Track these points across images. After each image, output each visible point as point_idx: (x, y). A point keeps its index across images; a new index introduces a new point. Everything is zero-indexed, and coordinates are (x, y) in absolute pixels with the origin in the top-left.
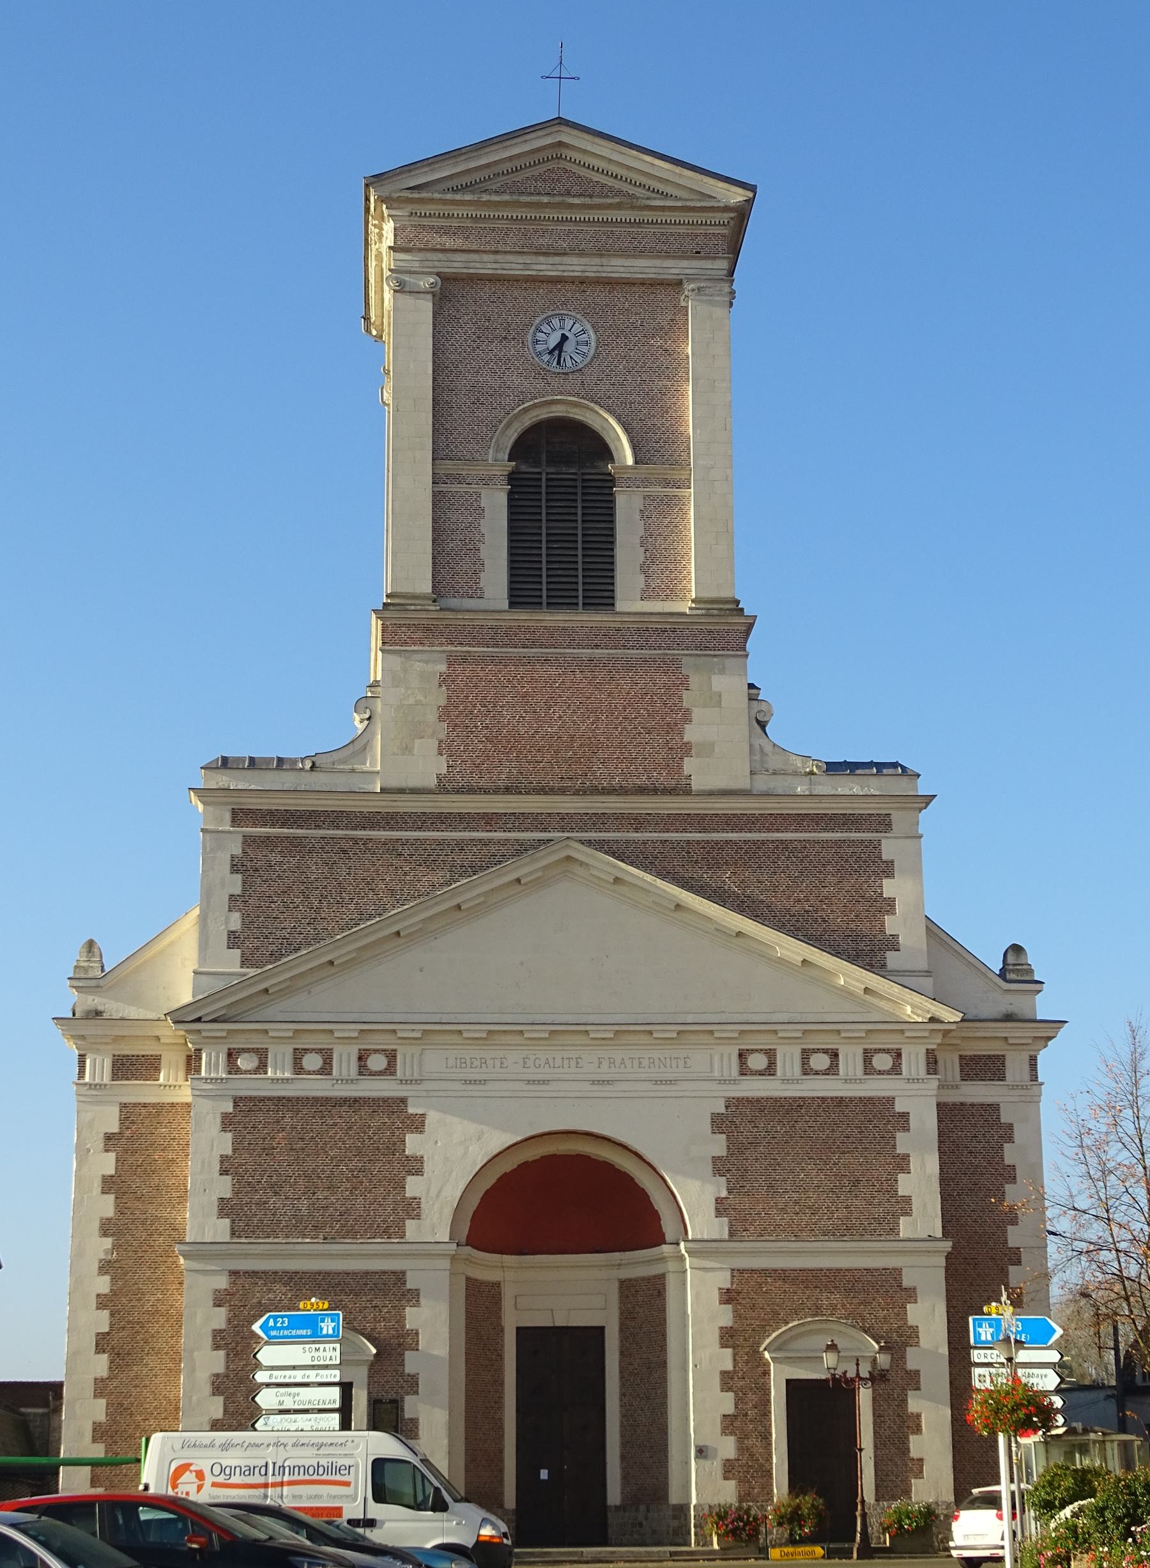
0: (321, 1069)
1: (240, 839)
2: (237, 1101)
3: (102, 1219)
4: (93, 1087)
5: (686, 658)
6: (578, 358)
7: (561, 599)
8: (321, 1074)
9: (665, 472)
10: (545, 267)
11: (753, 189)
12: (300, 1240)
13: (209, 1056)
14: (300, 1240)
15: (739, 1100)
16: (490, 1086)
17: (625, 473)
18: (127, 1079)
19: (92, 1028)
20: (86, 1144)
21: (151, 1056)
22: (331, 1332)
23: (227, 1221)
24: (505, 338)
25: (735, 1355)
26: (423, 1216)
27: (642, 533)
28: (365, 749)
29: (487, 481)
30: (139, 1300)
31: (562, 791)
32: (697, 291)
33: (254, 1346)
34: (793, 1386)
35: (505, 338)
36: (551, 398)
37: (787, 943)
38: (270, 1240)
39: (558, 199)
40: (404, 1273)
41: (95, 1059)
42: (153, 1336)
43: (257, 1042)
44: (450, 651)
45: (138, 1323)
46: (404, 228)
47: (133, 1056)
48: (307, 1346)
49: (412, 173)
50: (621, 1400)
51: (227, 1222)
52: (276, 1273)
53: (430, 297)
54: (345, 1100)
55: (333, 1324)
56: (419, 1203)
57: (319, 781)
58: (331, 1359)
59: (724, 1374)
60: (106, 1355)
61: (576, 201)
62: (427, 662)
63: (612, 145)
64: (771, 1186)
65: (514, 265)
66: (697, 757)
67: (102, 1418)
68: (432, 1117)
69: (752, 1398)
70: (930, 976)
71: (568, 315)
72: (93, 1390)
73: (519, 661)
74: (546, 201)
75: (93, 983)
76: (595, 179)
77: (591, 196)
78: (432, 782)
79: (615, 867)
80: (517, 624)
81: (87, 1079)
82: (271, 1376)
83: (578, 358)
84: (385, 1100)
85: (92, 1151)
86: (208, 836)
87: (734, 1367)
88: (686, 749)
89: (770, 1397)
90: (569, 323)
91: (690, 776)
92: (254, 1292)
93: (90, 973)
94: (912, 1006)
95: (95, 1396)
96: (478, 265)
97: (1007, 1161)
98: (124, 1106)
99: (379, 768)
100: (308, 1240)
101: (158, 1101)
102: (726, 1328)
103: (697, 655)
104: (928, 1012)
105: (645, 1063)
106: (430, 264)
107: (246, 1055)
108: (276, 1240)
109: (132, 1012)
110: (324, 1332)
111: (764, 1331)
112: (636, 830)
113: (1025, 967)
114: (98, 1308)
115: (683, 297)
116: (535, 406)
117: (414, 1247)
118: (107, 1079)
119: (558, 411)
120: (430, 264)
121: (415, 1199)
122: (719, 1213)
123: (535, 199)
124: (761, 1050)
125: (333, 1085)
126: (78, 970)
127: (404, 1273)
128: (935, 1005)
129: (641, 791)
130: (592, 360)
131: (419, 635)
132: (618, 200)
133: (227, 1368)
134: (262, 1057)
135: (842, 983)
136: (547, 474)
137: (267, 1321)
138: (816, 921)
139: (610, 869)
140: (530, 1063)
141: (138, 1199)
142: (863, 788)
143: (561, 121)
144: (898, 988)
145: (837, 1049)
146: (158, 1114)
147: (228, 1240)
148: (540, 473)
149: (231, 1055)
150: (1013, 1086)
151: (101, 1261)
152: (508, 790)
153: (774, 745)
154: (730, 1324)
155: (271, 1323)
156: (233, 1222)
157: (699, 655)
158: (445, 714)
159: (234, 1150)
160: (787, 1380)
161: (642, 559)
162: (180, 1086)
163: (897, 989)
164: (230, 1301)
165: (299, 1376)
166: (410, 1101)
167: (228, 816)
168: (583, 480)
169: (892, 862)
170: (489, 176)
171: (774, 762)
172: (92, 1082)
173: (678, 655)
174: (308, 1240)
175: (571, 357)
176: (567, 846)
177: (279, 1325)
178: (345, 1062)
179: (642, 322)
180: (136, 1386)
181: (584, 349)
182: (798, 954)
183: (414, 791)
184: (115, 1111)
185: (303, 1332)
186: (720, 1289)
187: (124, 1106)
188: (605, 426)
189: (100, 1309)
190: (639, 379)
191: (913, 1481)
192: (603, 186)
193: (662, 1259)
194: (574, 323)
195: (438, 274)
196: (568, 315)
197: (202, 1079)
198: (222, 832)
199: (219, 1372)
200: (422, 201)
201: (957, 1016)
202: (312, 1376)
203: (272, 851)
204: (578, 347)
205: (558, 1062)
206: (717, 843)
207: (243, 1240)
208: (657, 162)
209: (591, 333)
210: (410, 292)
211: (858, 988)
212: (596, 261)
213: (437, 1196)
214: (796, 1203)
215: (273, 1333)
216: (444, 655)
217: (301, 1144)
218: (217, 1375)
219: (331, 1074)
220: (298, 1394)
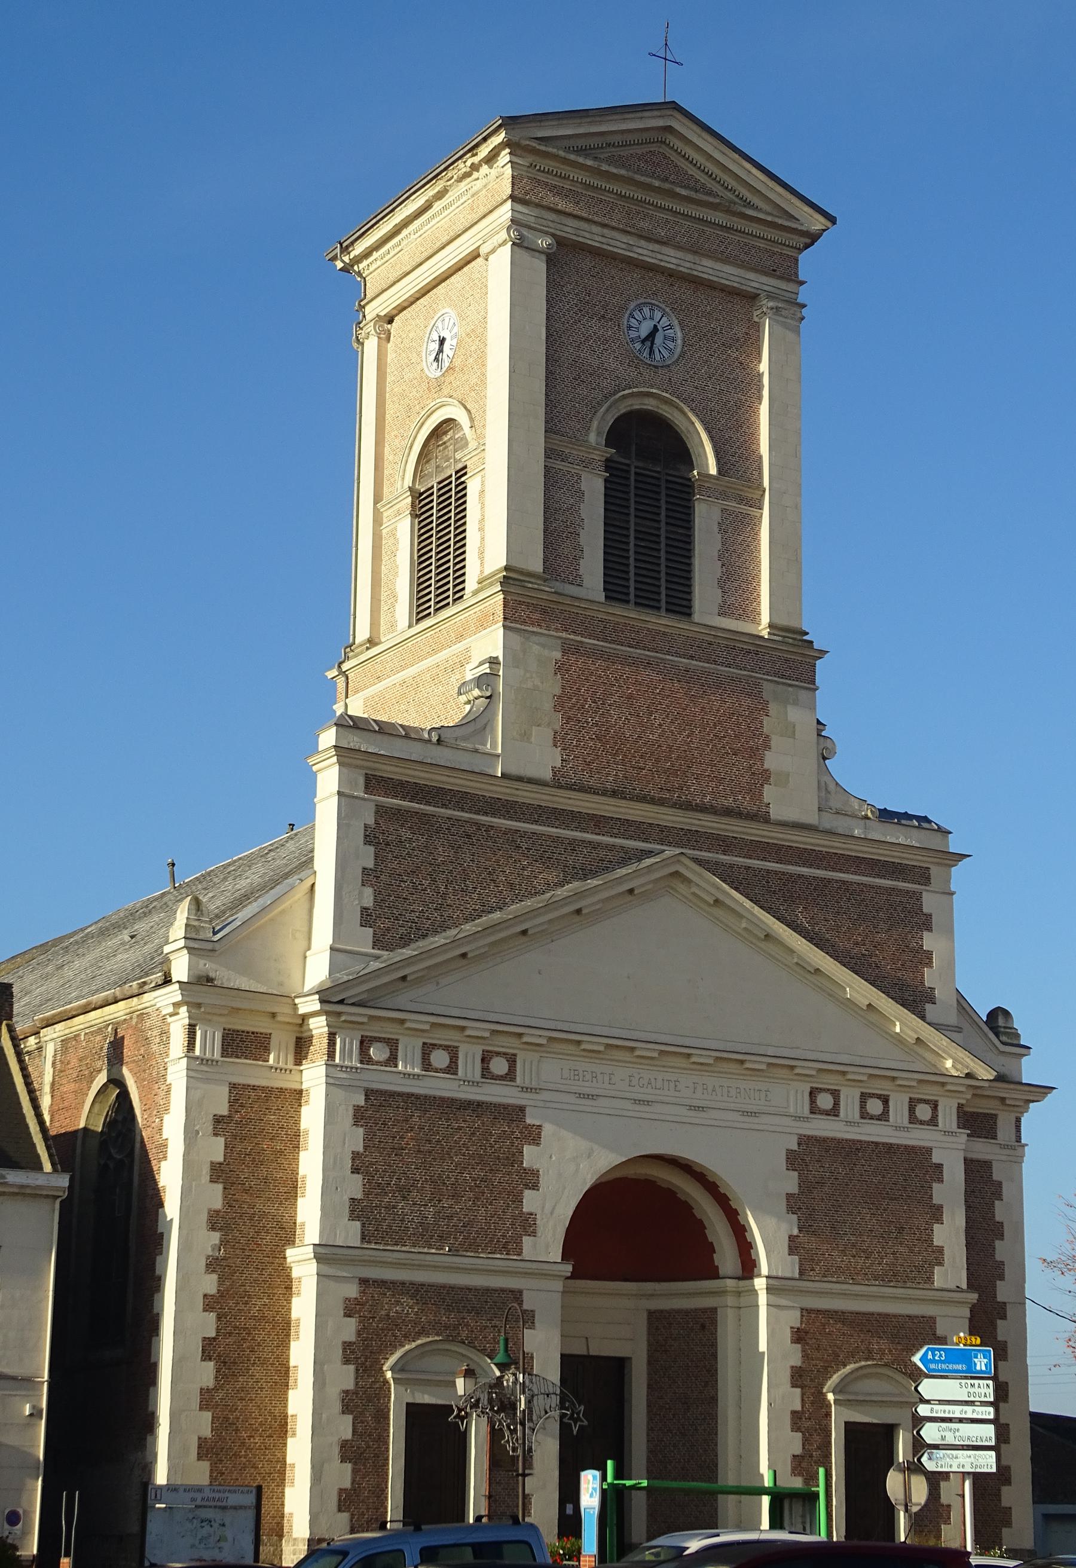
0: (447, 1067)
1: (372, 808)
2: (369, 1093)
3: (210, 1210)
4: (204, 1062)
5: (769, 683)
6: (666, 353)
7: (647, 601)
8: (448, 1073)
9: (741, 488)
10: (645, 252)
11: (833, 220)
12: (426, 1250)
13: (343, 1043)
14: (426, 1250)
15: (809, 1138)
16: (602, 1102)
17: (707, 481)
18: (237, 1057)
19: (206, 996)
20: (194, 1126)
21: (261, 1034)
22: (984, 1368)
23: (358, 1224)
24: (603, 317)
25: (803, 1394)
26: (539, 1234)
27: (719, 546)
28: (485, 728)
29: (586, 464)
30: (246, 1303)
31: (661, 802)
32: (775, 310)
33: (383, 1361)
34: (852, 1430)
35: (603, 317)
36: (647, 390)
37: (859, 986)
38: (398, 1248)
39: (667, 186)
40: (521, 1292)
41: (206, 1032)
42: (259, 1345)
43: (389, 1031)
44: (565, 639)
45: (245, 1329)
46: (521, 178)
47: (243, 1032)
48: (964, 1381)
49: (542, 124)
50: (648, 1435)
51: (358, 1224)
52: (403, 1283)
53: (544, 257)
54: (470, 1103)
55: (986, 1360)
56: (535, 1219)
57: (442, 756)
58: (985, 1396)
59: (793, 1413)
60: (212, 1363)
61: (684, 192)
62: (543, 646)
63: (716, 142)
64: (833, 1227)
65: (619, 244)
66: (775, 786)
67: (207, 1433)
68: (548, 1130)
69: (817, 1439)
70: (960, 1032)
71: (657, 306)
72: (199, 1401)
73: (626, 660)
74: (657, 185)
75: (209, 946)
76: (690, 172)
77: (696, 191)
78: (548, 775)
79: (718, 888)
80: (623, 621)
81: (197, 1052)
82: (932, 1410)
83: (666, 353)
84: (506, 1107)
85: (200, 1134)
86: (343, 799)
87: (802, 1408)
88: (766, 776)
89: (831, 1439)
90: (658, 315)
91: (769, 804)
92: (383, 1303)
93: (201, 933)
94: (955, 1060)
95: (201, 1409)
96: (587, 235)
97: (997, 1219)
98: (233, 1086)
99: (500, 752)
100: (433, 1251)
101: (267, 1085)
102: (796, 1367)
103: (775, 681)
104: (967, 1067)
105: (733, 1092)
106: (545, 223)
107: (379, 1044)
108: (404, 1249)
109: (244, 983)
110: (978, 1368)
111: (826, 1373)
112: (724, 853)
113: (1013, 1031)
114: (205, 1310)
115: (759, 312)
116: (632, 395)
117: (534, 1266)
118: (217, 1055)
119: (650, 404)
120: (545, 223)
121: (532, 1214)
122: (792, 1250)
123: (648, 180)
124: (828, 1090)
125: (459, 1086)
126: (188, 929)
127: (521, 1292)
128: (974, 1062)
129: (728, 812)
130: (678, 359)
131: (536, 616)
132: (718, 201)
133: (356, 1385)
134: (392, 1045)
135: (898, 1030)
136: (636, 467)
137: (926, 1354)
138: (870, 965)
139: (713, 891)
140: (635, 1082)
141: (246, 1191)
142: (907, 839)
143: (674, 106)
144: (947, 1042)
145: (888, 1096)
146: (267, 1099)
147: (359, 1246)
148: (628, 465)
149: (365, 1044)
150: (1004, 1145)
151: (208, 1257)
152: (614, 794)
153: (837, 784)
154: (799, 1364)
155: (930, 1356)
156: (363, 1225)
157: (778, 683)
158: (560, 703)
159: (365, 1147)
160: (845, 1423)
161: (719, 574)
162: (291, 1071)
163: (945, 1041)
164: (360, 1311)
165: (957, 1411)
166: (528, 1110)
167: (361, 781)
168: (667, 481)
169: (931, 915)
170: (602, 144)
171: (835, 803)
172: (202, 1056)
173: (761, 679)
174: (433, 1251)
175: (660, 351)
176: (679, 861)
177: (937, 1358)
178: (469, 1064)
179: (721, 329)
180: (242, 1399)
181: (671, 345)
182: (866, 997)
183: (530, 781)
184: (225, 1090)
185: (959, 1367)
186: (791, 1328)
187: (233, 1086)
188: (691, 429)
189: (207, 1311)
190: (718, 387)
191: (942, 1526)
192: (697, 181)
193: (722, 1293)
194: (663, 316)
195: (553, 235)
196: (657, 306)
197: (337, 1066)
198: (356, 797)
199: (349, 1388)
200: (546, 155)
201: (991, 1074)
202: (969, 1412)
203: (402, 826)
204: (666, 342)
205: (659, 1084)
206: (791, 875)
207: (373, 1246)
208: (754, 171)
209: (678, 329)
210: (527, 248)
211: (910, 1037)
212: (689, 257)
213: (552, 1213)
214: (854, 1245)
215: (933, 1366)
216: (559, 642)
217: (428, 1147)
218: (346, 1392)
219: (457, 1074)
220: (958, 1430)
